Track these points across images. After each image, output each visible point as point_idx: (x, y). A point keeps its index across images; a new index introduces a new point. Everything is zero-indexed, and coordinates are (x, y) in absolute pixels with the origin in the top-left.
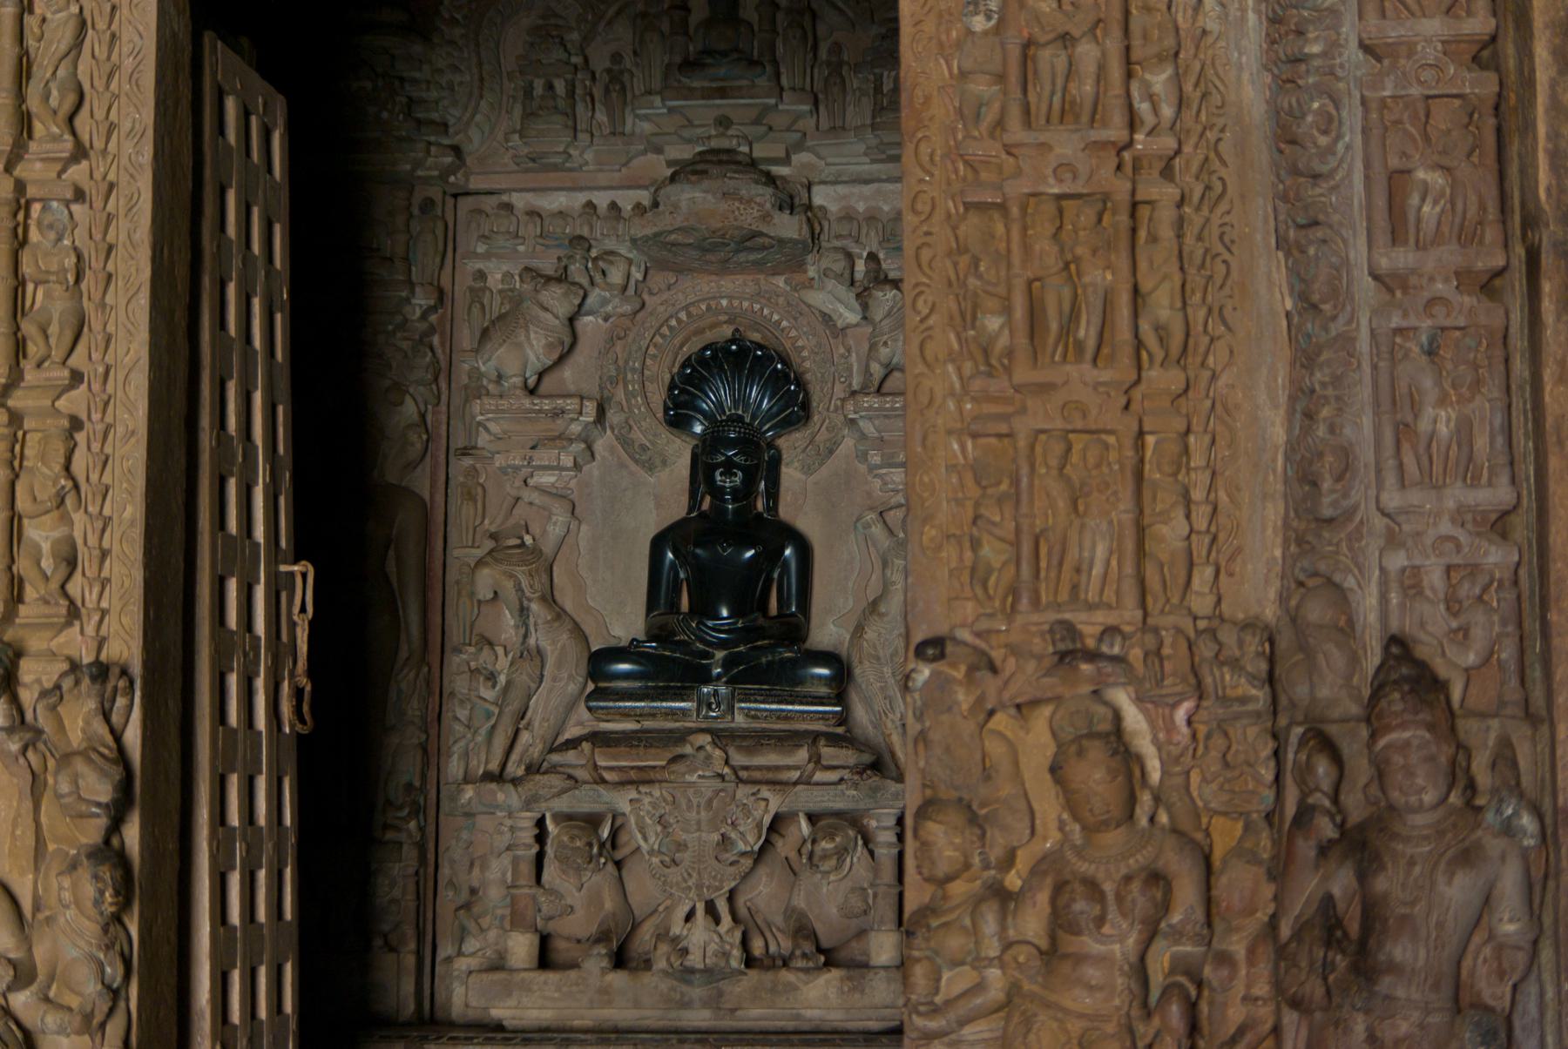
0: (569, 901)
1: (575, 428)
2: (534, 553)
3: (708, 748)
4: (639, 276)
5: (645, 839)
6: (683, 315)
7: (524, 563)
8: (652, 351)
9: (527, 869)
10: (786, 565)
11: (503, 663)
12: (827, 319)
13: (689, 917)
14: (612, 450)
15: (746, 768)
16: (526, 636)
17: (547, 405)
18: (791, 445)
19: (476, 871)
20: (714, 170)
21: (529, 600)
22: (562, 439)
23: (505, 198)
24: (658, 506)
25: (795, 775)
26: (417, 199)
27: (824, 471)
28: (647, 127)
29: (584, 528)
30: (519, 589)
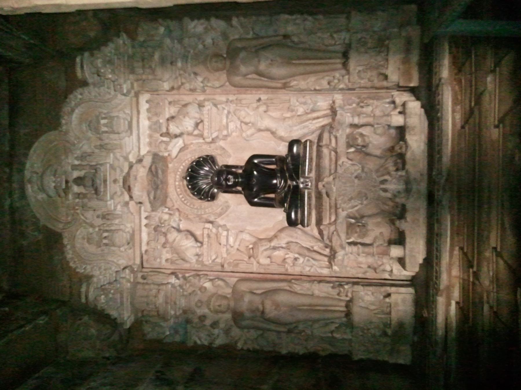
0: (378, 234)
1: (214, 230)
2: (255, 244)
3: (324, 183)
4: (167, 210)
5: (356, 206)
6: (181, 196)
7: (258, 248)
8: (192, 206)
9: (367, 249)
10: (260, 162)
11: (291, 255)
12: (181, 150)
13: (385, 190)
14: (223, 219)
15: (330, 170)
16: (282, 248)
17: (206, 240)
18: (222, 161)
19: (362, 266)
20: (128, 183)
21: (270, 246)
22: (218, 236)
23: (143, 252)
24: (240, 204)
25: (333, 153)
26: (141, 281)
27: (230, 151)
28: (119, 207)
29: (247, 228)
30: (266, 250)
